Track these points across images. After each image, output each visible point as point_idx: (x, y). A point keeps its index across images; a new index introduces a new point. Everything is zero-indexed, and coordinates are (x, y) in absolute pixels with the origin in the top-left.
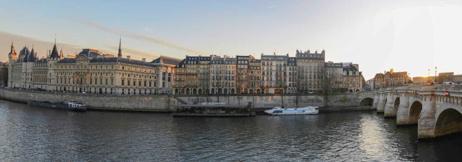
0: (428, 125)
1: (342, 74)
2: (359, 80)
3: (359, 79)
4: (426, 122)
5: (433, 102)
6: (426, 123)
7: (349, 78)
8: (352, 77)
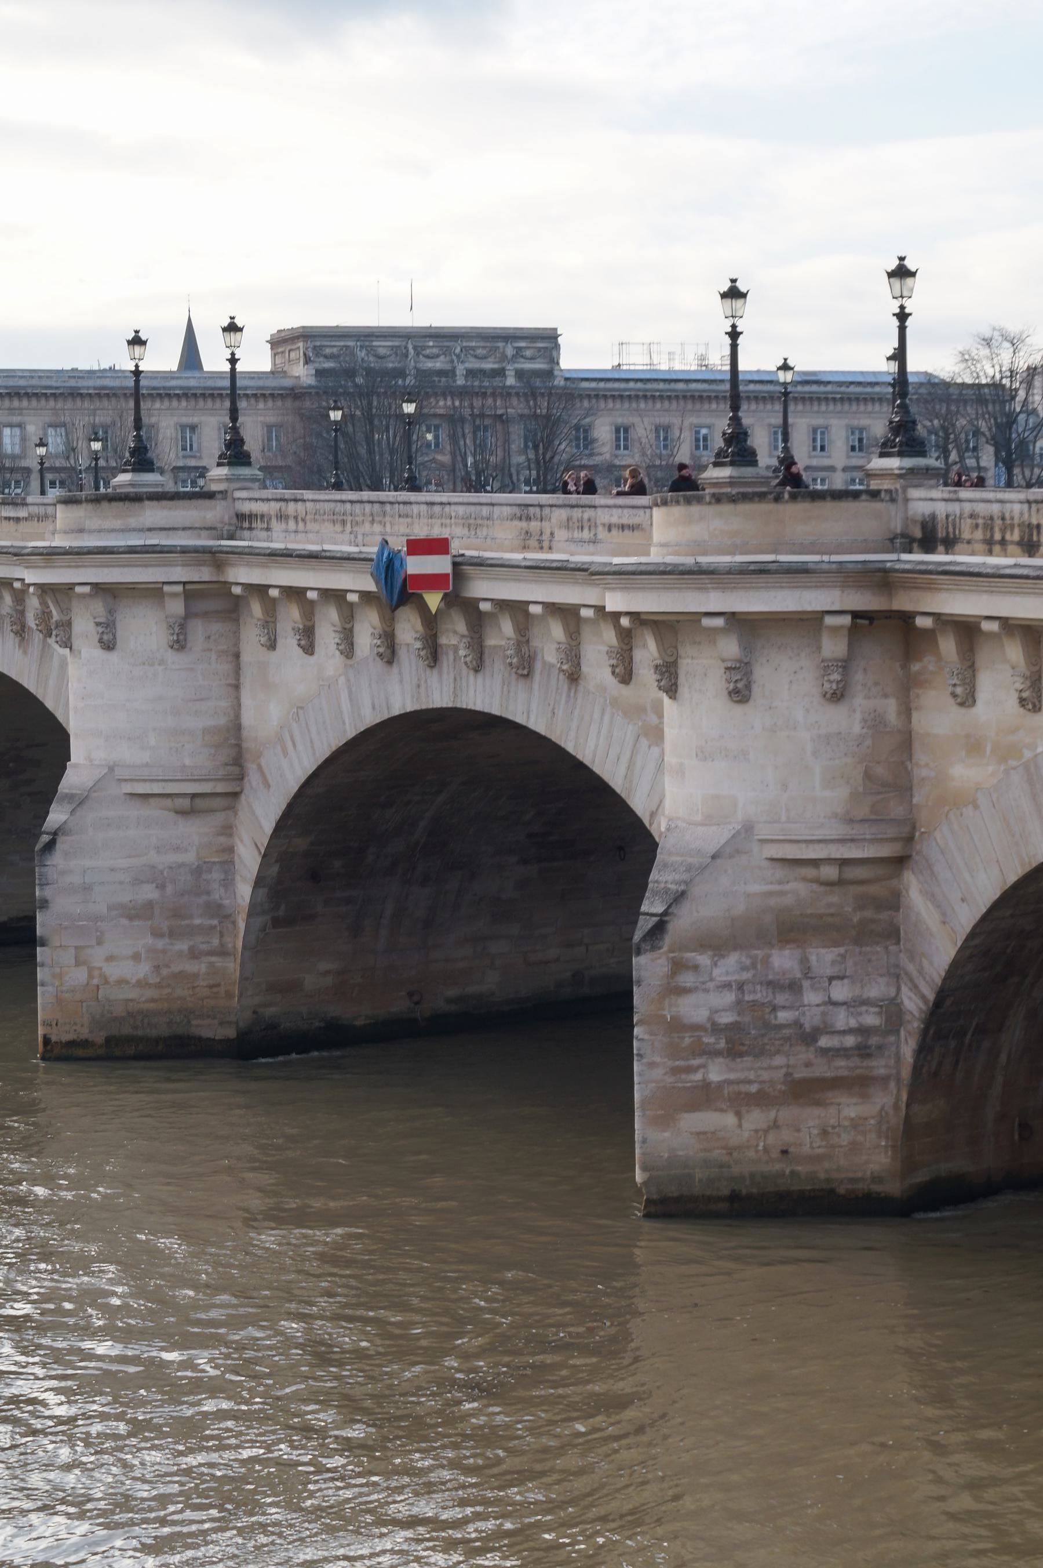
0: (797, 1024)
4: (761, 995)
5: (876, 723)
6: (754, 1005)
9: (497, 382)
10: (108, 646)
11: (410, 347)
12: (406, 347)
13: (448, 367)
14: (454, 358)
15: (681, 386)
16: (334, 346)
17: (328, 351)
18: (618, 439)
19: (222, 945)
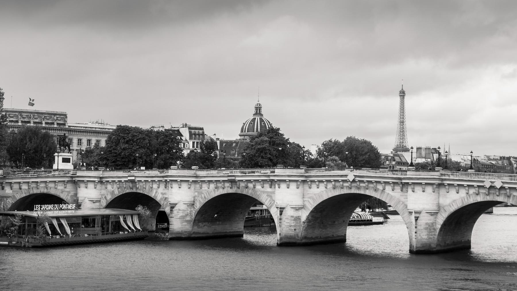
9: (52, 126)
10: (413, 191)
11: (32, 115)
12: (31, 116)
13: (40, 121)
14: (42, 119)
15: (94, 129)
16: (13, 114)
17: (11, 115)
18: (78, 142)
19: (435, 234)
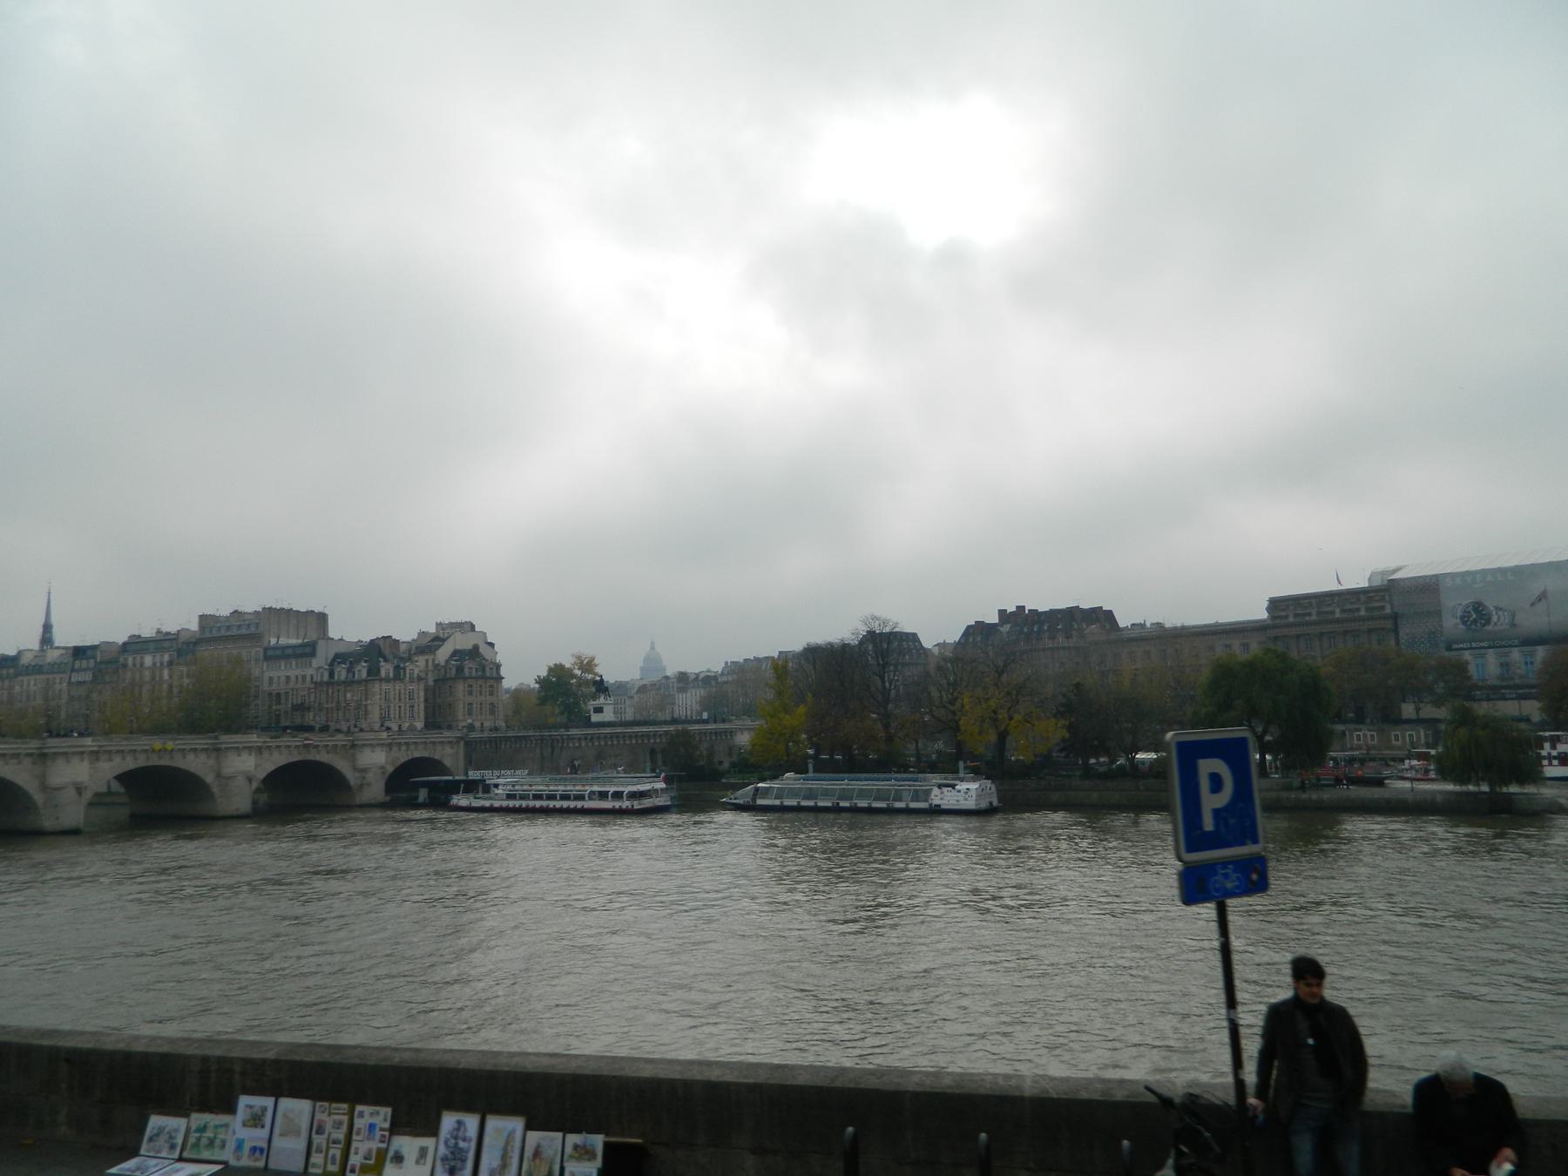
1: (315, 679)
2: (366, 695)
3: (366, 690)
7: (333, 689)
8: (342, 687)
